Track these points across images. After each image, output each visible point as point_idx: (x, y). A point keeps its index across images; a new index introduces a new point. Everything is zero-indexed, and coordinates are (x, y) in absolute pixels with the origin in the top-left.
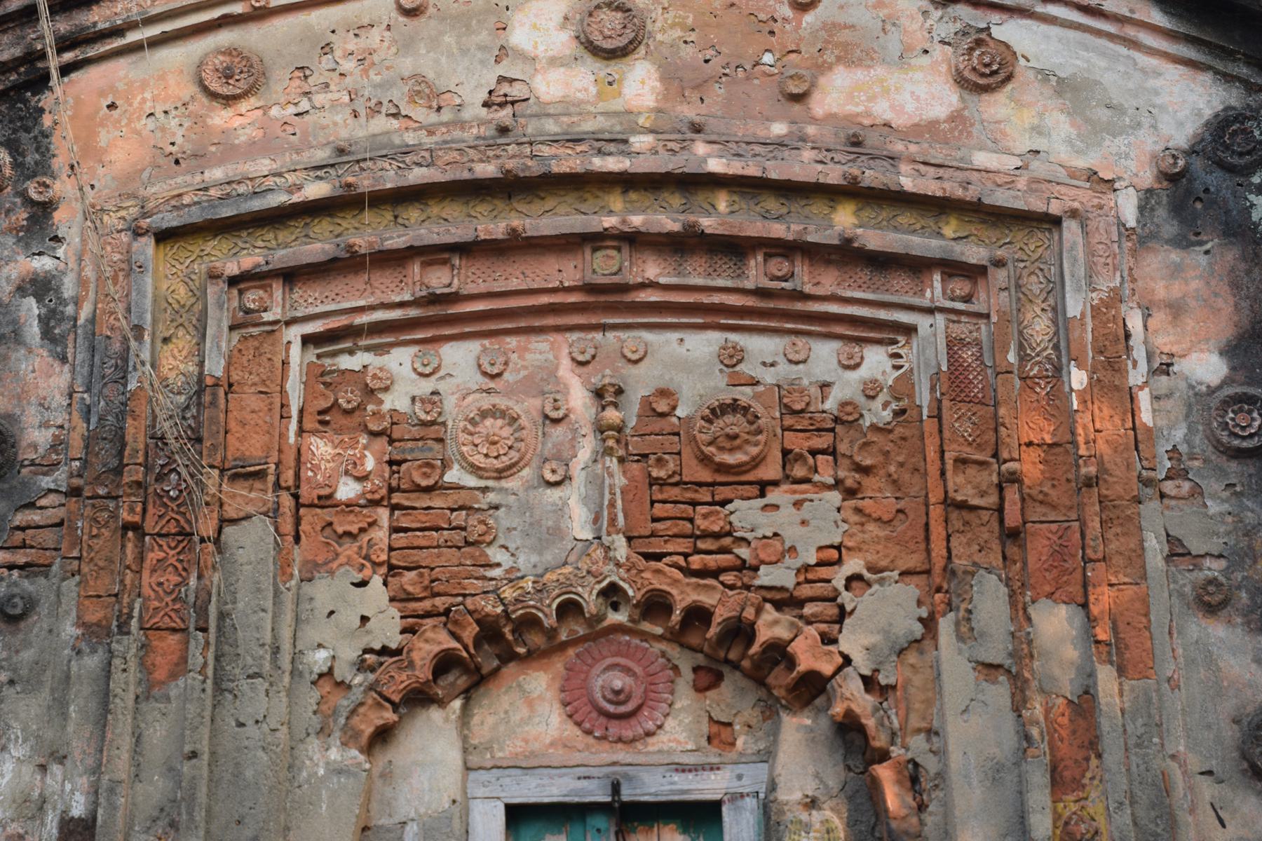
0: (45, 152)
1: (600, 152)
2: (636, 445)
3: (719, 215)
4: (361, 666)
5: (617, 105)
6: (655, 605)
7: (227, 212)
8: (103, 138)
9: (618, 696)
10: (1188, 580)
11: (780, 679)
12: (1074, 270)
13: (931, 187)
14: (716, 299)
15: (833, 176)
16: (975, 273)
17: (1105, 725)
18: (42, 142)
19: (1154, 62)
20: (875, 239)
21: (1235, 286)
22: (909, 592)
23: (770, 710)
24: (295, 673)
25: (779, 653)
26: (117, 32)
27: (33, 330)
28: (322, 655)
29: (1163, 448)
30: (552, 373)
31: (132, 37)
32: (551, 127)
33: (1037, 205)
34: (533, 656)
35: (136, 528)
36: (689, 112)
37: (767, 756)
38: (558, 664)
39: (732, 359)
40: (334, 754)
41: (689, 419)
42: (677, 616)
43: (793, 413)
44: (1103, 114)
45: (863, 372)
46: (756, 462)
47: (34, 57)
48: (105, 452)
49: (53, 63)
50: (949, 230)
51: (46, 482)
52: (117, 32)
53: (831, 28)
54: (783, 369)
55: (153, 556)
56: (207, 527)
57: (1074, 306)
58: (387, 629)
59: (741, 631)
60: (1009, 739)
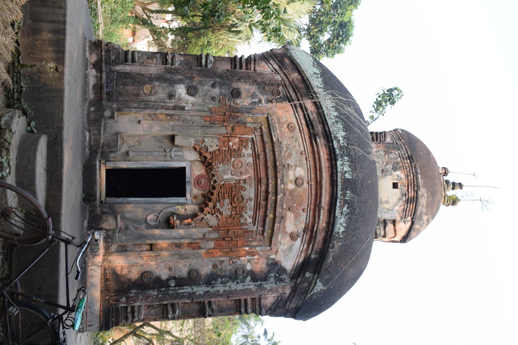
0: (280, 102)
1: (281, 180)
2: (237, 185)
3: (271, 197)
4: (205, 146)
5: (288, 183)
6: (214, 188)
7: (271, 127)
8: (282, 110)
9: (201, 183)
10: (218, 263)
11: (203, 206)
12: (263, 248)
13: (275, 228)
14: (259, 197)
15: (277, 214)
16: (263, 234)
17: (197, 250)
18: (281, 102)
19: (294, 260)
20: (268, 220)
21: (261, 271)
22: (216, 224)
23: (199, 204)
24: (204, 137)
25: (207, 205)
26: (297, 112)
27: (254, 101)
28: (207, 140)
29: (237, 261)
30: (248, 173)
31: (296, 114)
32: (285, 173)
33: (273, 243)
34: (207, 170)
35: (225, 114)
36: (287, 193)
37: (192, 204)
38: (205, 174)
39: (250, 199)
40: (193, 142)
41: (241, 193)
42: (212, 191)
43: (243, 208)
44: (286, 253)
45: (248, 218)
46: (235, 203)
47: (293, 101)
48: (236, 110)
49: (292, 103)
50: (269, 231)
51: (232, 103)
52: (297, 112)
53: (300, 214)
54: (249, 207)
55: (221, 117)
56: (225, 124)
57: (258, 248)
58: (210, 150)
59: (210, 200)
60: (194, 237)
